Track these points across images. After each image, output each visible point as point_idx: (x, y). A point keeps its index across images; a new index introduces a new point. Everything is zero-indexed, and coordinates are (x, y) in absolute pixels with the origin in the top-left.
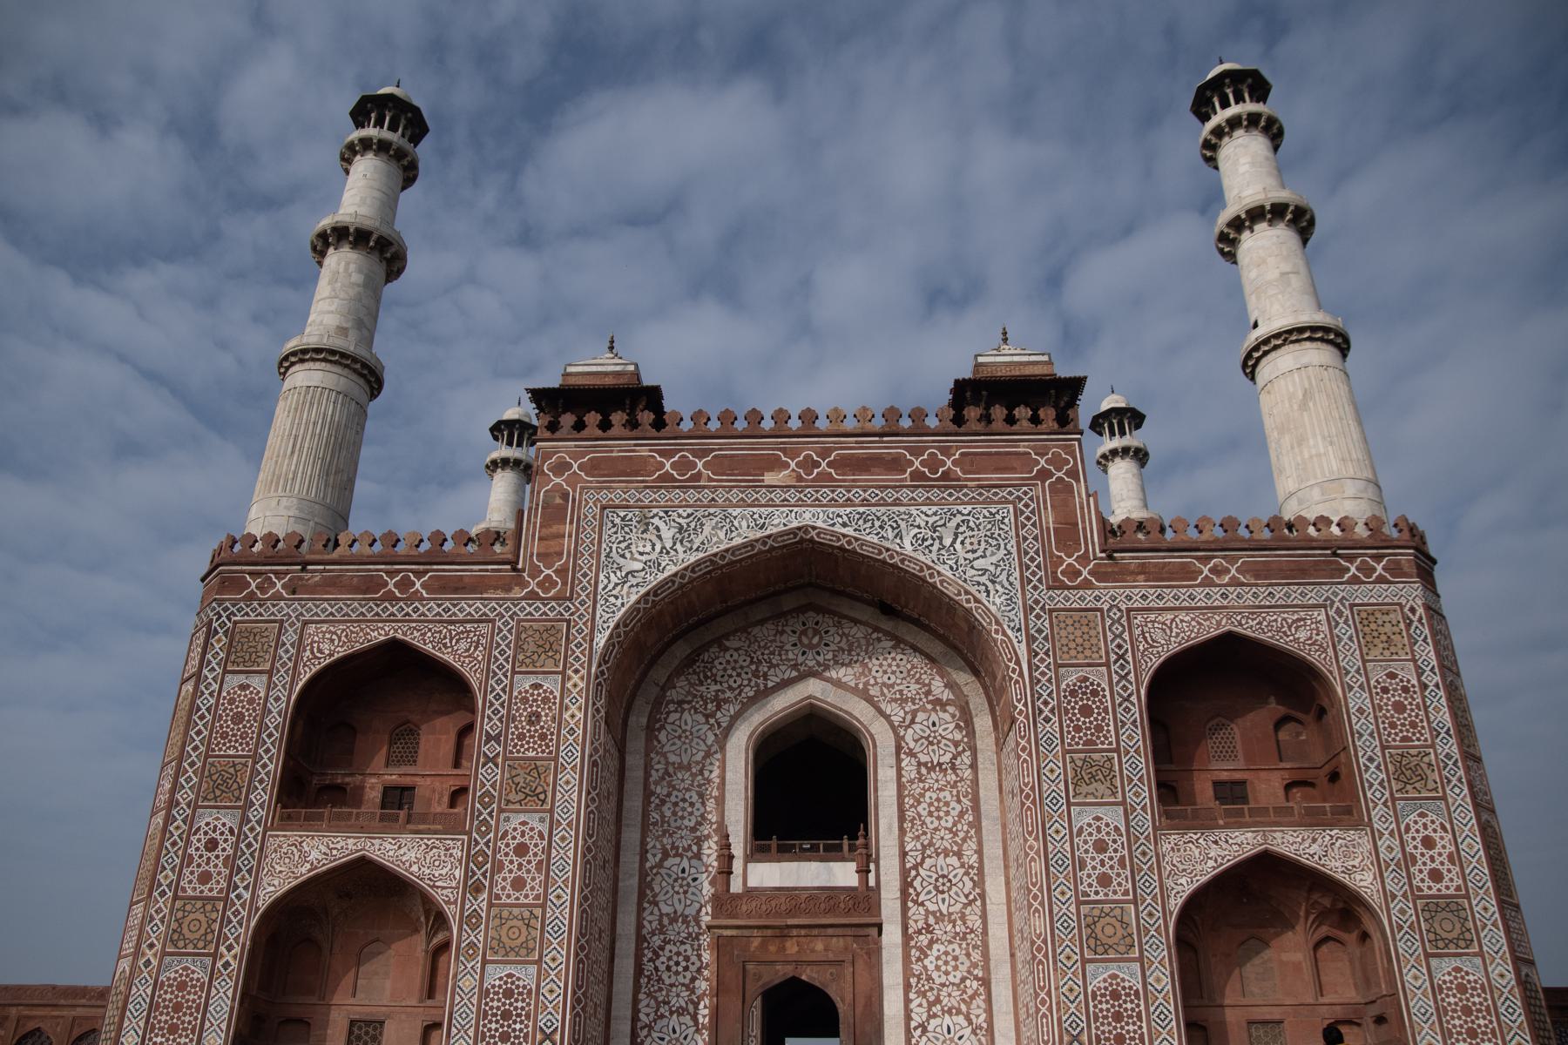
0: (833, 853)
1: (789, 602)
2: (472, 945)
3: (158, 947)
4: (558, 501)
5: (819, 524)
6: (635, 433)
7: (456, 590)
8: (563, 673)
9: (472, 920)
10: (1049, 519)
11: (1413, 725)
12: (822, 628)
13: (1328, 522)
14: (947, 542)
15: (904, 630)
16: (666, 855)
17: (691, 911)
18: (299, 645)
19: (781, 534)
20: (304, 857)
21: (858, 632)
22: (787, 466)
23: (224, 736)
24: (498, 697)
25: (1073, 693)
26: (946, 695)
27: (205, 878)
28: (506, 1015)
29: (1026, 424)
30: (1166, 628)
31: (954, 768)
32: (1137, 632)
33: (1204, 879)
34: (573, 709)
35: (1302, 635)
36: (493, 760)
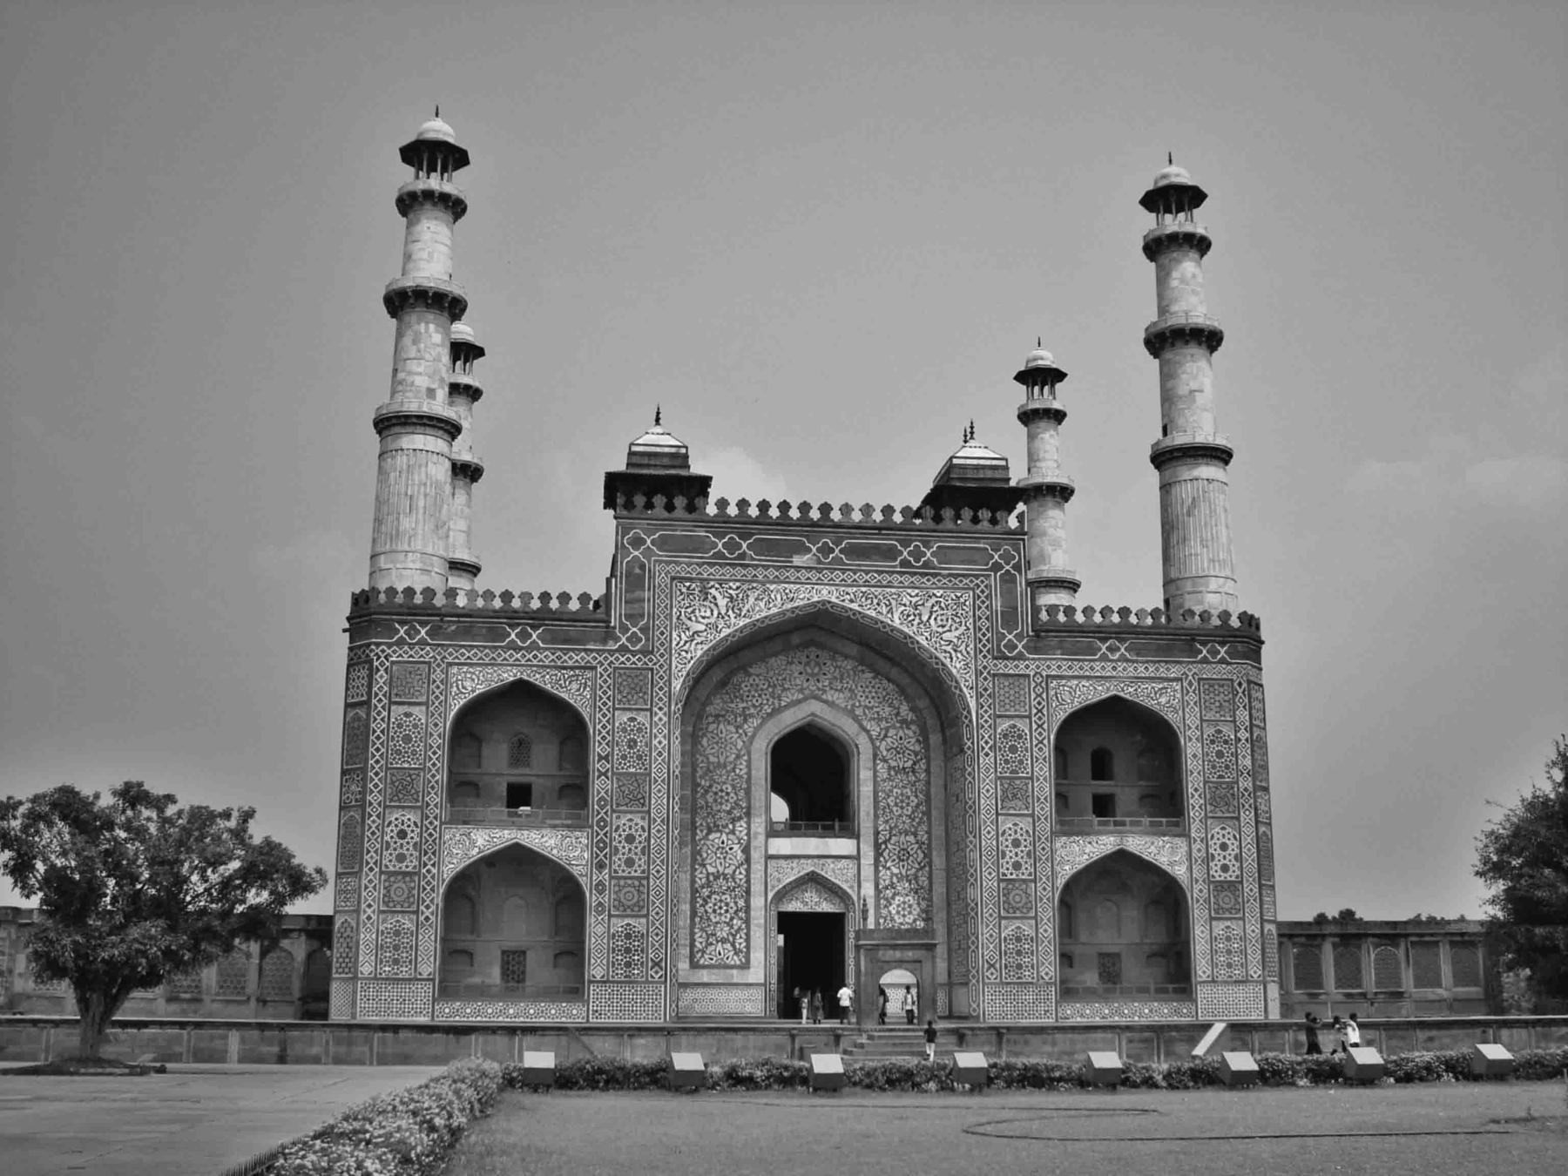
0: (828, 832)
1: (796, 639)
2: (600, 904)
3: (375, 907)
4: (637, 571)
5: (833, 600)
6: (693, 516)
7: (565, 642)
8: (650, 710)
9: (600, 887)
10: (998, 604)
11: (1227, 767)
12: (821, 660)
13: (1192, 613)
14: (925, 618)
15: (881, 664)
16: (710, 831)
17: (729, 871)
18: (445, 682)
19: (805, 606)
20: (473, 843)
21: (848, 665)
22: (809, 550)
23: (398, 752)
24: (604, 727)
25: (1005, 736)
26: (910, 716)
27: (401, 858)
28: (628, 950)
29: (985, 525)
30: (1072, 691)
31: (914, 771)
32: (1052, 693)
33: (1080, 867)
34: (660, 737)
35: (1163, 700)
36: (605, 774)
